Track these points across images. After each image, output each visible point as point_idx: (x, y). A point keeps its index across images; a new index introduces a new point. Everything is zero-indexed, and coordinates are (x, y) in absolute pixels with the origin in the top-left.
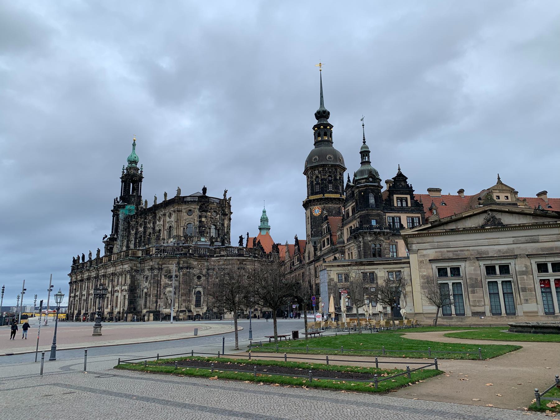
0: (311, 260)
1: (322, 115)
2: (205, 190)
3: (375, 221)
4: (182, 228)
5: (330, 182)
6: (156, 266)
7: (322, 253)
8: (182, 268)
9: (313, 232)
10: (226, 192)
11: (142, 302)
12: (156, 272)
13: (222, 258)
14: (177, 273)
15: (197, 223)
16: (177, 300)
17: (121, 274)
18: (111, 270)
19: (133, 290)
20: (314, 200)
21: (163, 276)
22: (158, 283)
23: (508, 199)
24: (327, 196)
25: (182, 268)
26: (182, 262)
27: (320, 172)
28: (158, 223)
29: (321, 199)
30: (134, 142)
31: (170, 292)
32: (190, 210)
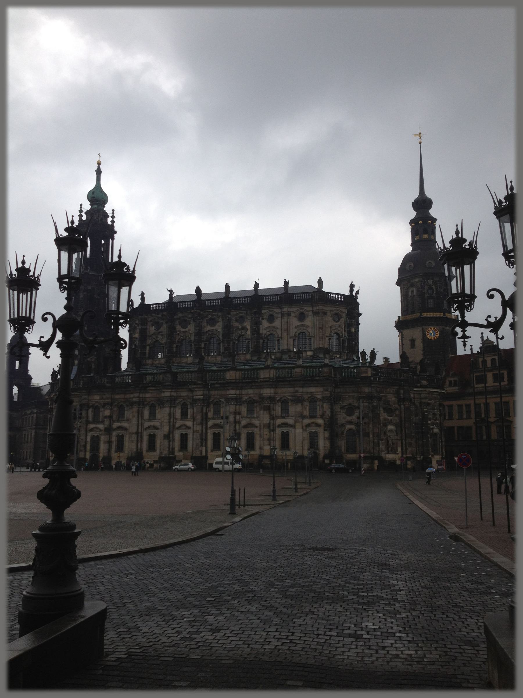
4: (327, 339)
11: (342, 443)
13: (428, 390)
14: (397, 406)
15: (344, 334)
16: (399, 443)
17: (299, 400)
19: (331, 425)
26: (402, 391)
28: (265, 324)
30: (99, 168)
31: (391, 431)
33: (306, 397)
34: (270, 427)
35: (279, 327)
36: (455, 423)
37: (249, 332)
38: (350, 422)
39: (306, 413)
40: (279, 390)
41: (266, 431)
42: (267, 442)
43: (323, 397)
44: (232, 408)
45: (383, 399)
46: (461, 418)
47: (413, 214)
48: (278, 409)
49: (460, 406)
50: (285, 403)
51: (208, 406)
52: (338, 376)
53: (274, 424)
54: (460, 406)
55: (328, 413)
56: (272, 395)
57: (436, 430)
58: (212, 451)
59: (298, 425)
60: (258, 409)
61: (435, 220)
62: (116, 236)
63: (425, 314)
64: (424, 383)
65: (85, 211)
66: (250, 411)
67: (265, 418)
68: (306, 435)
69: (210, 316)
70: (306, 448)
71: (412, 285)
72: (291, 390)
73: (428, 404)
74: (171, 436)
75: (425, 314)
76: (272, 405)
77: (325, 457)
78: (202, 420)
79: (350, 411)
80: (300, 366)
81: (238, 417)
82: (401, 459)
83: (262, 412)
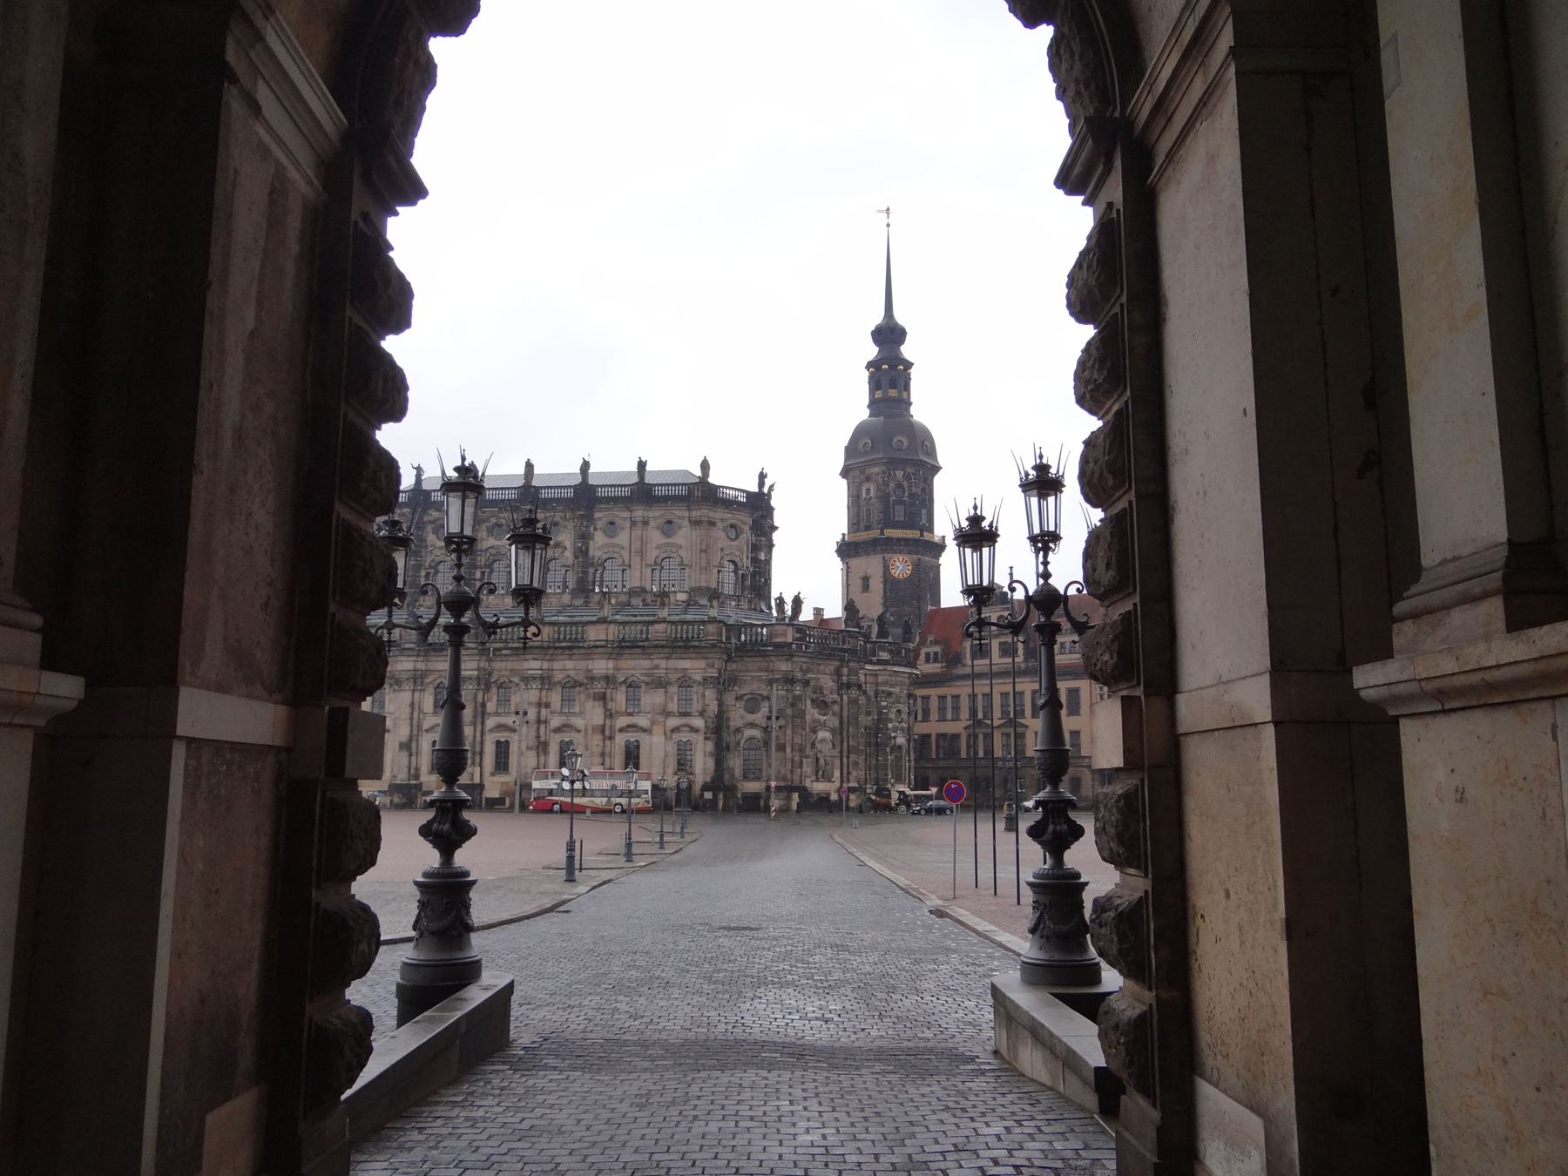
1: (889, 335)
8: (849, 686)
12: (798, 690)
14: (836, 697)
15: (746, 562)
16: (837, 762)
17: (660, 684)
19: (718, 729)
20: (899, 540)
22: (801, 714)
25: (849, 686)
26: (845, 671)
27: (907, 477)
28: (599, 539)
29: (916, 541)
31: (823, 740)
33: (673, 677)
34: (606, 733)
35: (626, 544)
36: (933, 728)
37: (569, 554)
38: (752, 725)
39: (673, 706)
40: (623, 664)
41: (596, 740)
42: (598, 760)
43: (705, 679)
44: (533, 695)
45: (813, 683)
46: (942, 719)
47: (872, 351)
48: (620, 698)
49: (942, 698)
50: (631, 685)
51: (488, 688)
52: (733, 641)
54: (942, 698)
55: (713, 707)
57: (901, 740)
58: (493, 774)
59: (657, 729)
60: (583, 697)
61: (909, 365)
63: (889, 533)
64: (885, 656)
66: (567, 701)
67: (596, 715)
68: (672, 748)
69: (493, 520)
70: (670, 771)
71: (868, 479)
72: (646, 663)
73: (890, 694)
74: (414, 745)
75: (889, 533)
77: (705, 788)
78: (475, 717)
79: (753, 704)
80: (664, 621)
81: (544, 712)
82: (839, 791)
83: (590, 703)
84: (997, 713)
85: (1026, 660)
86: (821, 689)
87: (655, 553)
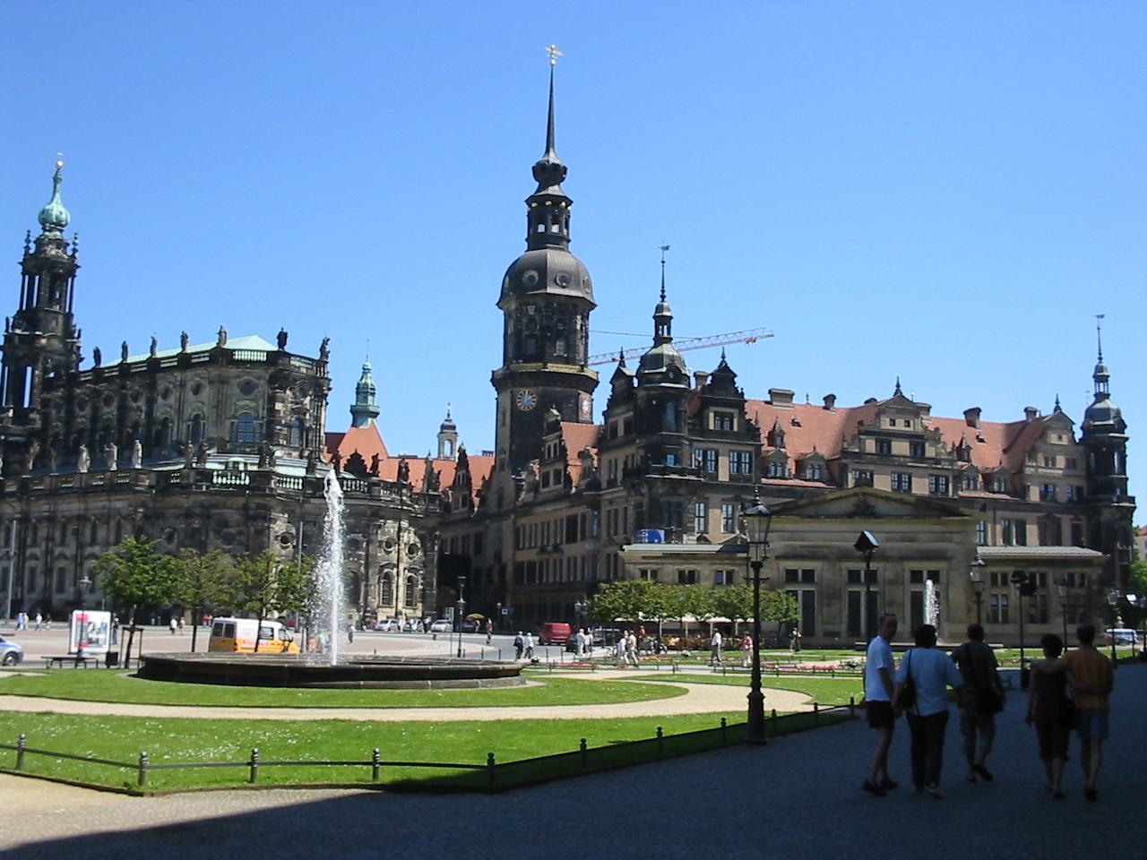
0: (505, 508)
1: (548, 173)
2: (282, 338)
3: (672, 456)
5: (559, 335)
6: (197, 511)
7: (541, 497)
9: (514, 447)
10: (325, 342)
14: (242, 528)
18: (72, 507)
21: (212, 534)
23: (909, 426)
24: (552, 367)
27: (538, 310)
28: (160, 400)
32: (248, 383)
39: (112, 539)
53: (81, 555)
56: (82, 512)
62: (78, 271)
65: (32, 239)
76: (81, 528)
81: (50, 545)
84: (552, 542)
85: (565, 487)
86: (226, 524)
87: (189, 411)
